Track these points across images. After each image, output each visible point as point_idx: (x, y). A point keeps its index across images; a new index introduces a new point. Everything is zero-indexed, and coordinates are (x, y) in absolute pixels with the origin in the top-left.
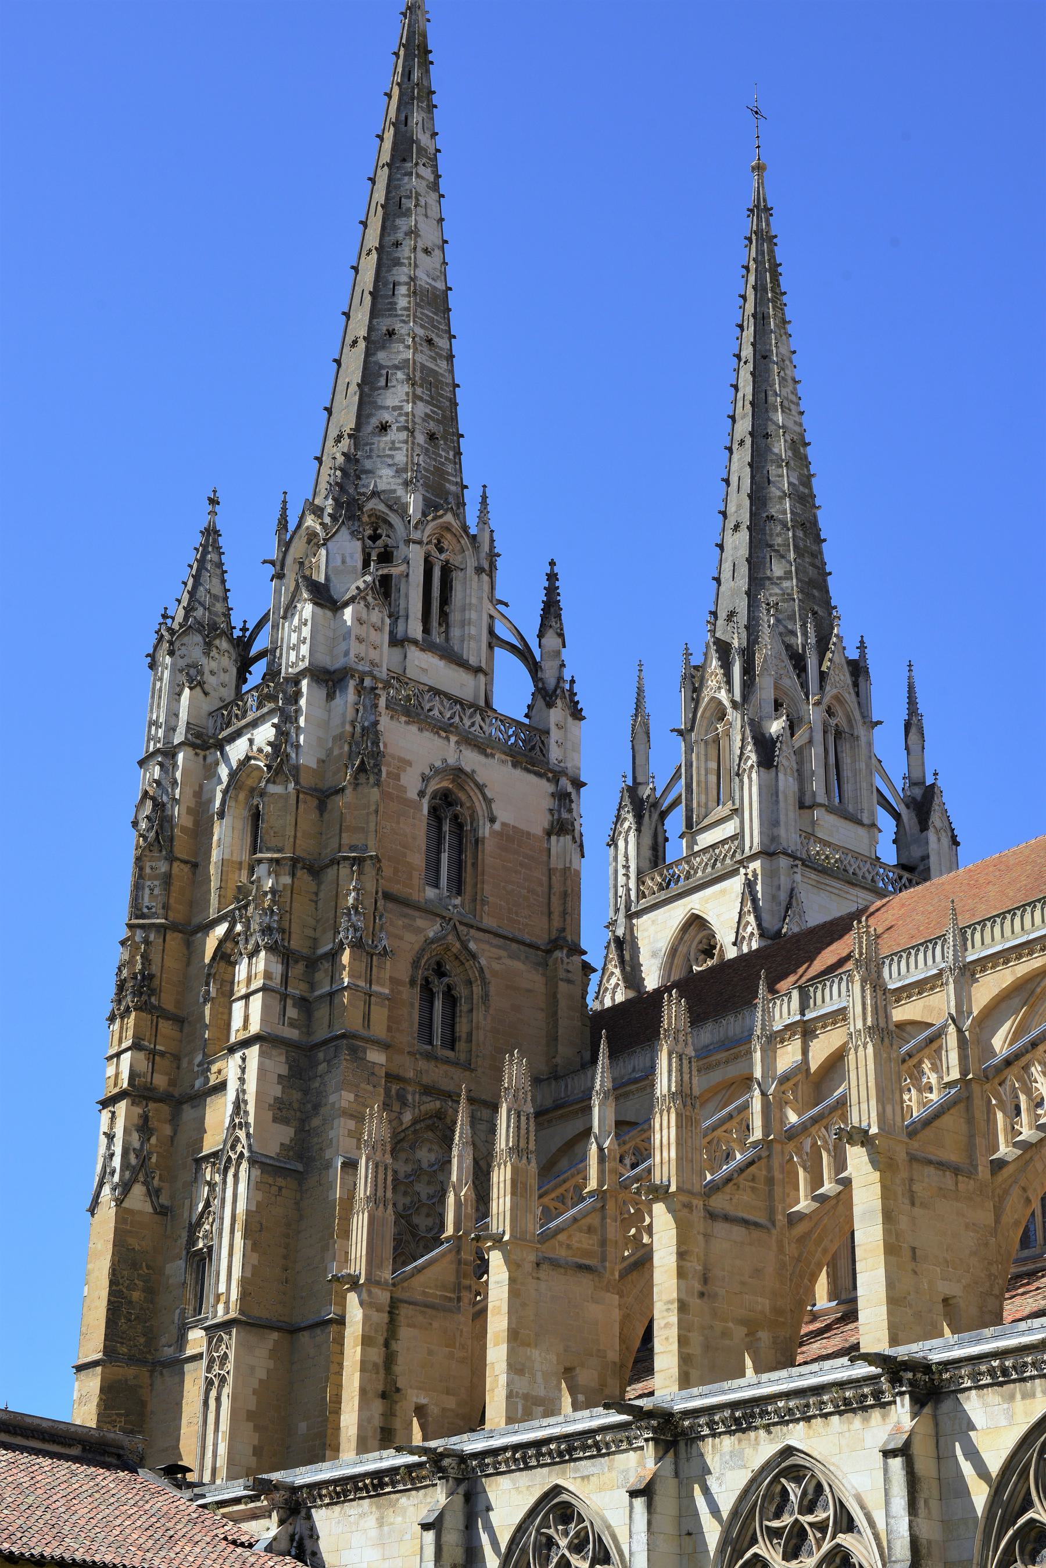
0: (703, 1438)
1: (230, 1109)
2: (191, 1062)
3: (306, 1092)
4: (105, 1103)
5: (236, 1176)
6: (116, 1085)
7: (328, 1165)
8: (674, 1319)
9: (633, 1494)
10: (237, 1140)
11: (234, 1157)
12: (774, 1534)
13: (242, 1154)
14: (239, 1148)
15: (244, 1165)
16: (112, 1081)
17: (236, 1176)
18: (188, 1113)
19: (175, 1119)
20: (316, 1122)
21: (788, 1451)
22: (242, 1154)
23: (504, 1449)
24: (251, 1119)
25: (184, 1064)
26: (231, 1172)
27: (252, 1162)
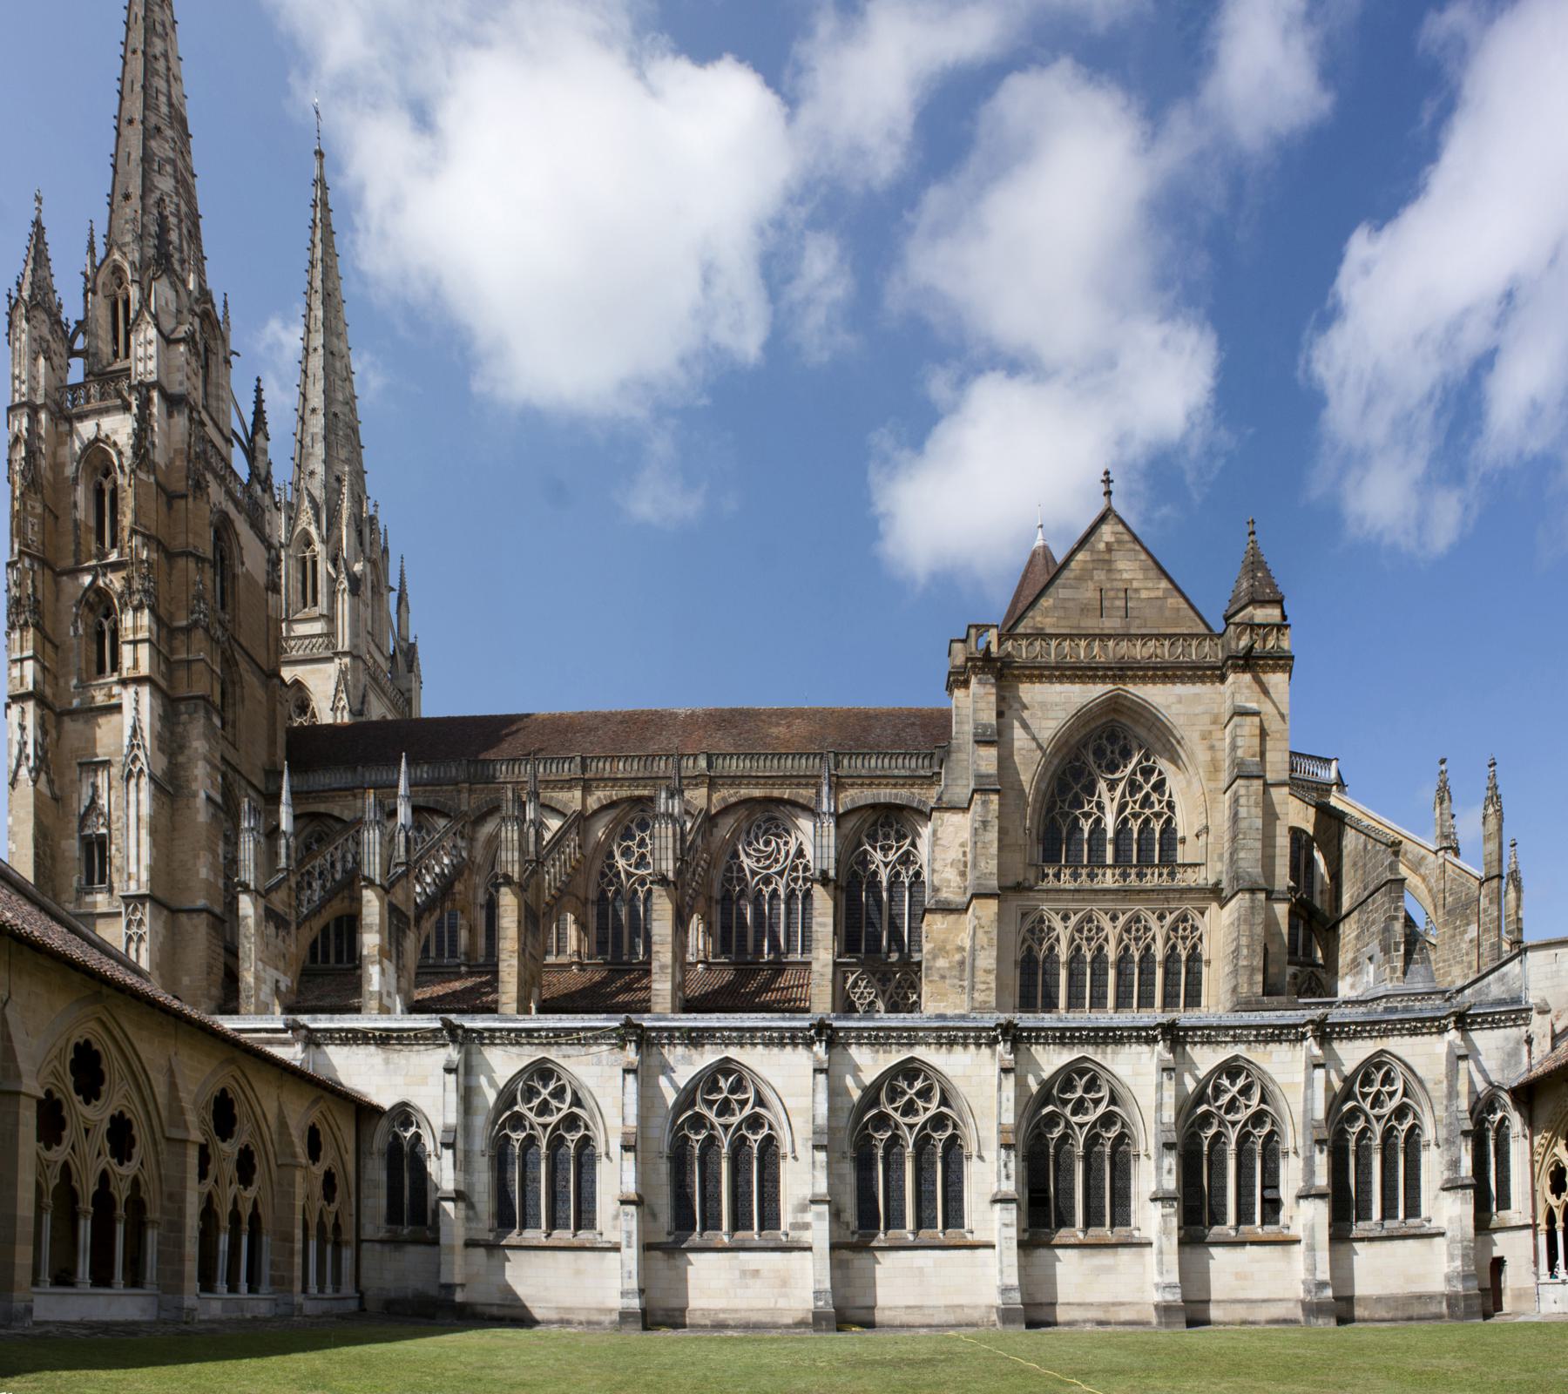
0: (663, 1046)
1: (128, 732)
2: (67, 683)
3: (172, 733)
4: (16, 698)
5: (137, 785)
6: (22, 684)
7: (195, 795)
8: (515, 962)
9: (626, 1071)
10: (136, 758)
11: (135, 770)
12: (710, 1104)
13: (141, 770)
14: (138, 765)
15: (144, 781)
16: (18, 682)
17: (137, 785)
18: (69, 725)
19: (59, 726)
20: (181, 759)
21: (727, 1060)
22: (141, 770)
23: (501, 1030)
24: (148, 744)
25: (62, 682)
26: (133, 782)
27: (152, 778)
